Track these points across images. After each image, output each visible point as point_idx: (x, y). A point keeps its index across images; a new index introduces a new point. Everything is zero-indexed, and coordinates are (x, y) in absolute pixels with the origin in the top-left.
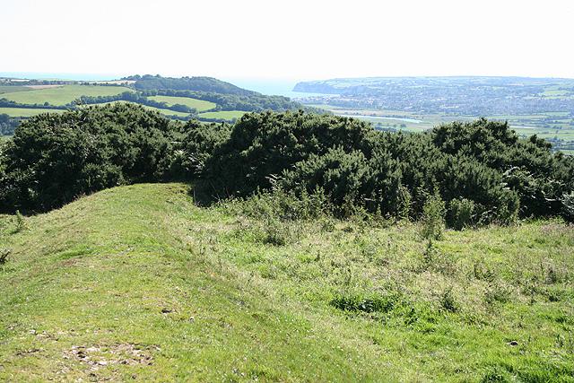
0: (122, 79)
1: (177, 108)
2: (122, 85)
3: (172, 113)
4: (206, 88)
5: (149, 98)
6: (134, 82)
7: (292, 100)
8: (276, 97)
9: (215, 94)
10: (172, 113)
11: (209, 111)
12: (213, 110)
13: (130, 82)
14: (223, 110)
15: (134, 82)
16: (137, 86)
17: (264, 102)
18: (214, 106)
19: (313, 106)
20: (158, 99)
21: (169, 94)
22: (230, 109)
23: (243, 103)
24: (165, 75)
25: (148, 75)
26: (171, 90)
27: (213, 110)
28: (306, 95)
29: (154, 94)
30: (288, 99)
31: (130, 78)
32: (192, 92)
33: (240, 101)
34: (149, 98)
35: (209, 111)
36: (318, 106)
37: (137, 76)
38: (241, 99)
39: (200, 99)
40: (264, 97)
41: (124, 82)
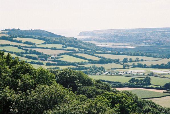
0: (2, 31)
1: (26, 43)
2: (2, 33)
3: (24, 45)
4: (38, 34)
5: (14, 39)
6: (7, 32)
7: (78, 39)
8: (71, 38)
9: (44, 37)
10: (24, 45)
11: (41, 44)
12: (43, 44)
13: (6, 32)
14: (48, 44)
15: (7, 32)
16: (8, 33)
17: (65, 40)
18: (44, 42)
19: (87, 42)
20: (18, 39)
21: (23, 37)
22: (51, 43)
23: (56, 40)
24: (21, 29)
25: (14, 29)
26: (24, 35)
27: (43, 44)
28: (85, 37)
29: (16, 37)
30: (76, 39)
31: (6, 30)
32: (33, 36)
33: (55, 40)
34: (14, 39)
35: (41, 44)
36: (89, 42)
37: (9, 30)
38: (56, 39)
39: (37, 39)
40: (66, 38)
41: (3, 32)
